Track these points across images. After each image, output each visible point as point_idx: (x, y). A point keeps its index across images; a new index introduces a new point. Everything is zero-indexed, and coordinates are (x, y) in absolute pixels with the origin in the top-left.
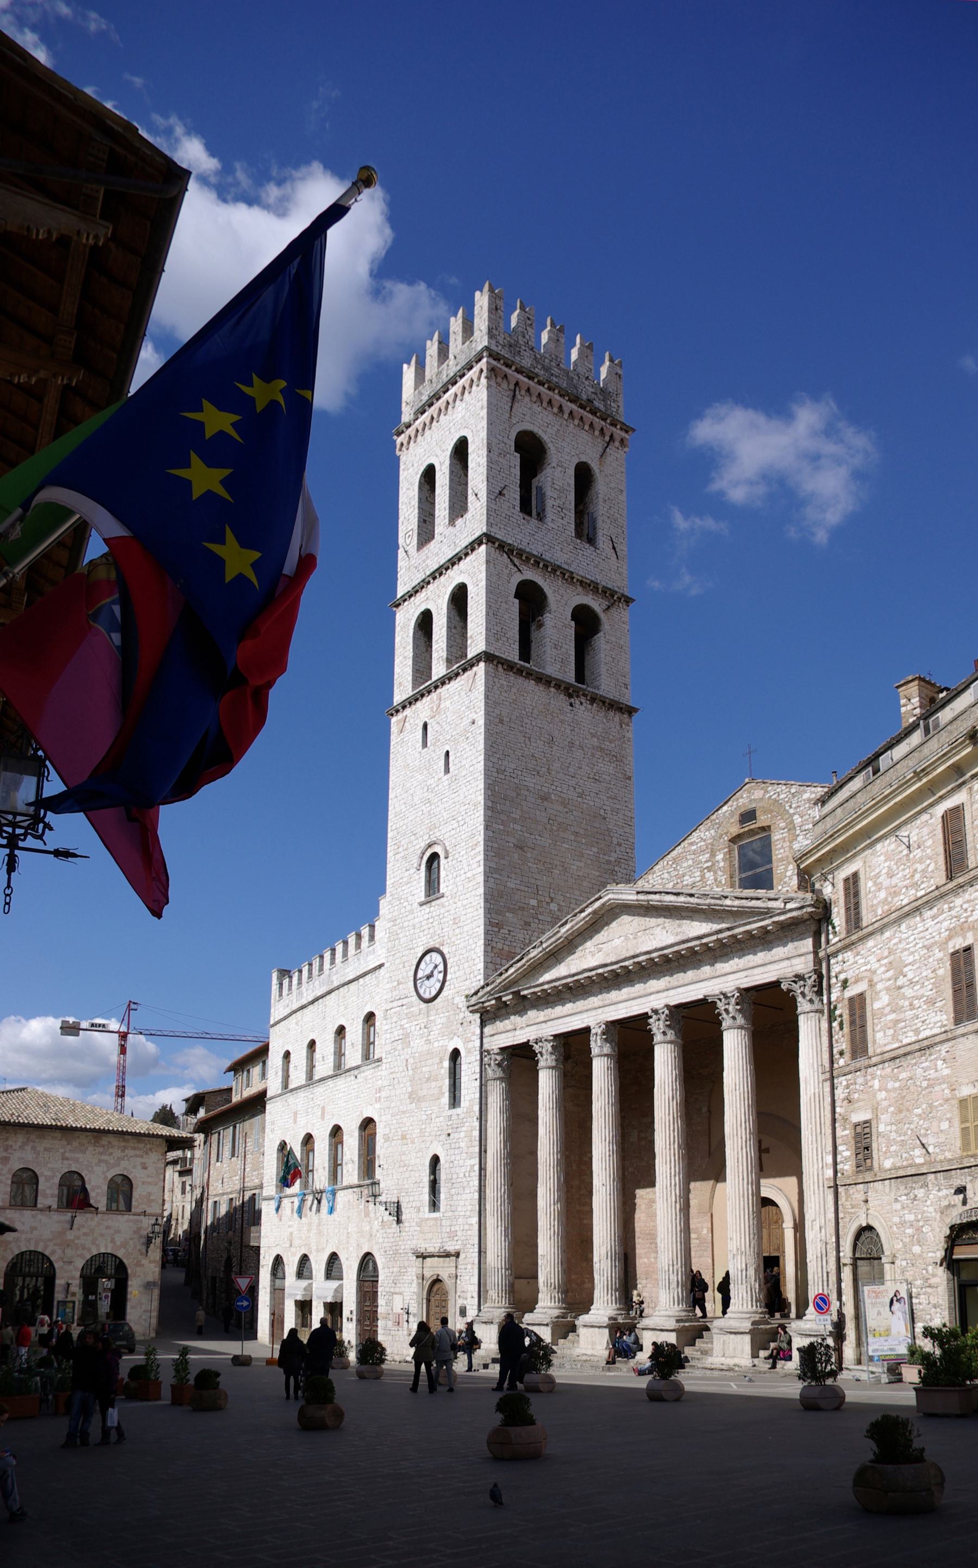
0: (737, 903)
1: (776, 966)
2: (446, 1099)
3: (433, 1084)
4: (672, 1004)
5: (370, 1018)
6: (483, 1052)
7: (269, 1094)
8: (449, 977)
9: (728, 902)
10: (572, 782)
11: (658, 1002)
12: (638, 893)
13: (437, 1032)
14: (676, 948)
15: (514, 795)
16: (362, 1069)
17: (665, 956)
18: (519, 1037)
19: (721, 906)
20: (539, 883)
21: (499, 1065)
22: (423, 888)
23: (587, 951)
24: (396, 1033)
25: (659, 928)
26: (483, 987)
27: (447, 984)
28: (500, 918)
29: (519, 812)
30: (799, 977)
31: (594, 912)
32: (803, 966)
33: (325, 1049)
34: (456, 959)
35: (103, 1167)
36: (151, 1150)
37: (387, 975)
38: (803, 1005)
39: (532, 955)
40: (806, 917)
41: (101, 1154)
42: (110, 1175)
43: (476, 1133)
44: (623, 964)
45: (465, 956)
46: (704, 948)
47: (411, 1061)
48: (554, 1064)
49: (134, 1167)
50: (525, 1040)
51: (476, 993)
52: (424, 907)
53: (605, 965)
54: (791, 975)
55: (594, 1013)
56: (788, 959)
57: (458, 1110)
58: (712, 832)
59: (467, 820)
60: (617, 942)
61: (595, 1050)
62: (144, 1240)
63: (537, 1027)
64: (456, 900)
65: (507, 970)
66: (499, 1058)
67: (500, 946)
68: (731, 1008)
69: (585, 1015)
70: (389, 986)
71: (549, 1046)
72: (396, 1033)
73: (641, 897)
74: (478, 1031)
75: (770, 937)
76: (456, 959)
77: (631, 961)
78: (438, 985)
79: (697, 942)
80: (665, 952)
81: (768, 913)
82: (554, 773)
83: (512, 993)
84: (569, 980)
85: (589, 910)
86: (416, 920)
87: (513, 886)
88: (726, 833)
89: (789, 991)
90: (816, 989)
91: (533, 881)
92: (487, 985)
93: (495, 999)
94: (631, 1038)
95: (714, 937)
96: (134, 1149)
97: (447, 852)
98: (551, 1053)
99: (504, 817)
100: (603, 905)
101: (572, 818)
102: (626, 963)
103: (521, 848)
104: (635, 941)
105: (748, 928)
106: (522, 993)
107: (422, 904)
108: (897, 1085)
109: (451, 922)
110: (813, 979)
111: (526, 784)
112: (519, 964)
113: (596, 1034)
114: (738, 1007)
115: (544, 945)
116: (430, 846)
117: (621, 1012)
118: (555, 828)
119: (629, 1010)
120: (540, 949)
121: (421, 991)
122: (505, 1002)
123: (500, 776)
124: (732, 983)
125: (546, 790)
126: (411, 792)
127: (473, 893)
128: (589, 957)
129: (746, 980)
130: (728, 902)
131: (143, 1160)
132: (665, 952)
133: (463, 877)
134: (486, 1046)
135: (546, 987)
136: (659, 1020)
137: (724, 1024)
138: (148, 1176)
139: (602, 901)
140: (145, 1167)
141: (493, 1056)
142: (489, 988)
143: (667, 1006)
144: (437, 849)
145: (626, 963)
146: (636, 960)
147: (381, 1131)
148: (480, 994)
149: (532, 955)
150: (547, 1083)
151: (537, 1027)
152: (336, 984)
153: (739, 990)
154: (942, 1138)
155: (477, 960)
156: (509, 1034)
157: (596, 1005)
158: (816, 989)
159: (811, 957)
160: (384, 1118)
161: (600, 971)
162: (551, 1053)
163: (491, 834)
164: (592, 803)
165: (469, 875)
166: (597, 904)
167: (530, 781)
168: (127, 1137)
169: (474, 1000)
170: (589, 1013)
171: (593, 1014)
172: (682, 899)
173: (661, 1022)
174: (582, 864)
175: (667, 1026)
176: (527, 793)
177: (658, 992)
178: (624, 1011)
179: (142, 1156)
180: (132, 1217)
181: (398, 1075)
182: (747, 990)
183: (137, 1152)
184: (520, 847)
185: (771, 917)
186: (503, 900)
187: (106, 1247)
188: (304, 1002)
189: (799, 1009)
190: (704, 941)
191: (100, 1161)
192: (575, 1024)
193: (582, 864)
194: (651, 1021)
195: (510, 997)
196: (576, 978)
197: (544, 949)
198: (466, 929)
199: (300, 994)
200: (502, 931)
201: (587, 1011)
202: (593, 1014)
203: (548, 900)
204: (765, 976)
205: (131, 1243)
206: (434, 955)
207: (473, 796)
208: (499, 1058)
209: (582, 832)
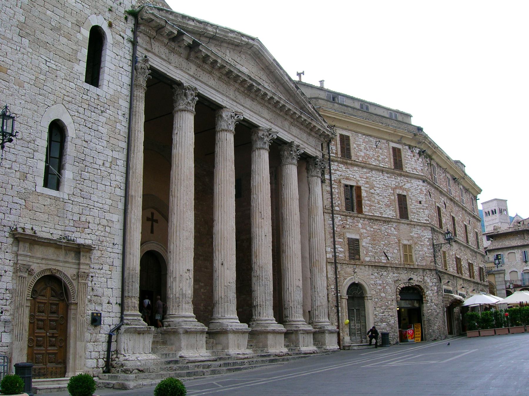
2: (82, 67)
3: (64, 40)
18: (175, 73)
19: (307, 105)
31: (247, 44)
50: (178, 79)
55: (231, 102)
69: (225, 98)
83: (194, 41)
84: (235, 72)
102: (269, 93)
105: (317, 125)
106: (200, 48)
108: (372, 229)
119: (251, 117)
135: (219, 61)
154: (394, 255)
156: (164, 63)
170: (228, 100)
178: (248, 115)
196: (239, 74)
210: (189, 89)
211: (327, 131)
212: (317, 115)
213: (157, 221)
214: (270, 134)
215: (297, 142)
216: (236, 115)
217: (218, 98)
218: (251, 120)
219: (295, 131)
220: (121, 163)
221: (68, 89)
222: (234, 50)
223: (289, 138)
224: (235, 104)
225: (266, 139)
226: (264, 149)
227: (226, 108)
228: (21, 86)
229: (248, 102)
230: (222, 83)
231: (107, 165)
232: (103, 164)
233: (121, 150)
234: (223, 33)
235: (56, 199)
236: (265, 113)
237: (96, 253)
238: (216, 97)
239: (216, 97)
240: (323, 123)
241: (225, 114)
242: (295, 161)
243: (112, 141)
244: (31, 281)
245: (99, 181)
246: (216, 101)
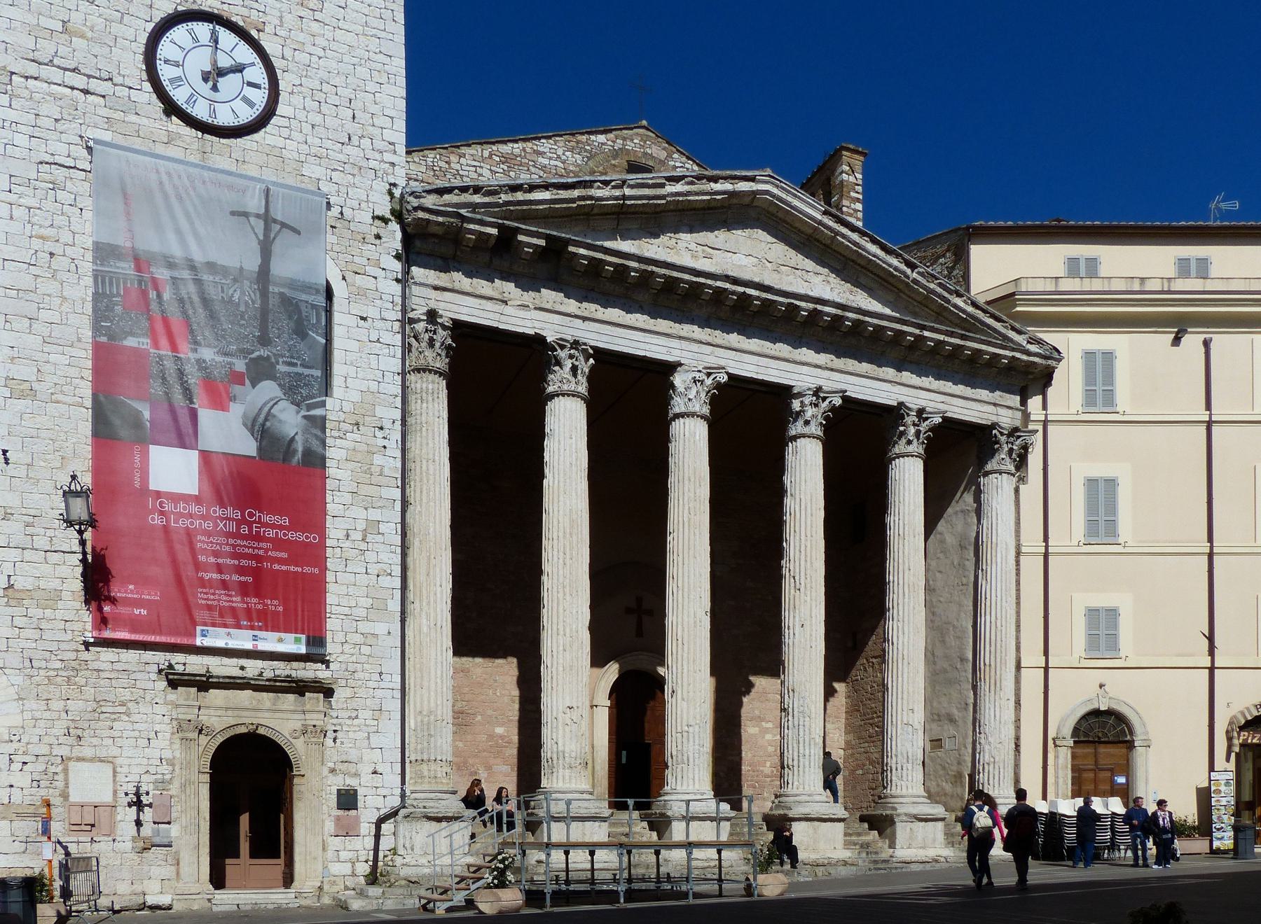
9: (959, 302)
19: (948, 301)
25: (821, 278)
55: (695, 347)
60: (740, 259)
69: (675, 343)
77: (811, 306)
79: (917, 331)
81: (1006, 342)
95: (941, 337)
104: (775, 275)
105: (984, 347)
130: (959, 302)
145: (803, 304)
146: (819, 307)
170: (685, 344)
190: (926, 334)
201: (680, 338)
210: (562, 347)
211: (1028, 353)
212: (990, 321)
214: (824, 399)
215: (914, 399)
216: (709, 375)
217: (654, 348)
218: (760, 377)
223: (894, 396)
225: (810, 412)
226: (804, 436)
227: (681, 365)
231: (359, 536)
232: (348, 536)
233: (389, 504)
238: (647, 347)
239: (647, 347)
240: (1012, 334)
241: (679, 380)
242: (916, 448)
243: (365, 490)
245: (341, 568)
246: (649, 354)
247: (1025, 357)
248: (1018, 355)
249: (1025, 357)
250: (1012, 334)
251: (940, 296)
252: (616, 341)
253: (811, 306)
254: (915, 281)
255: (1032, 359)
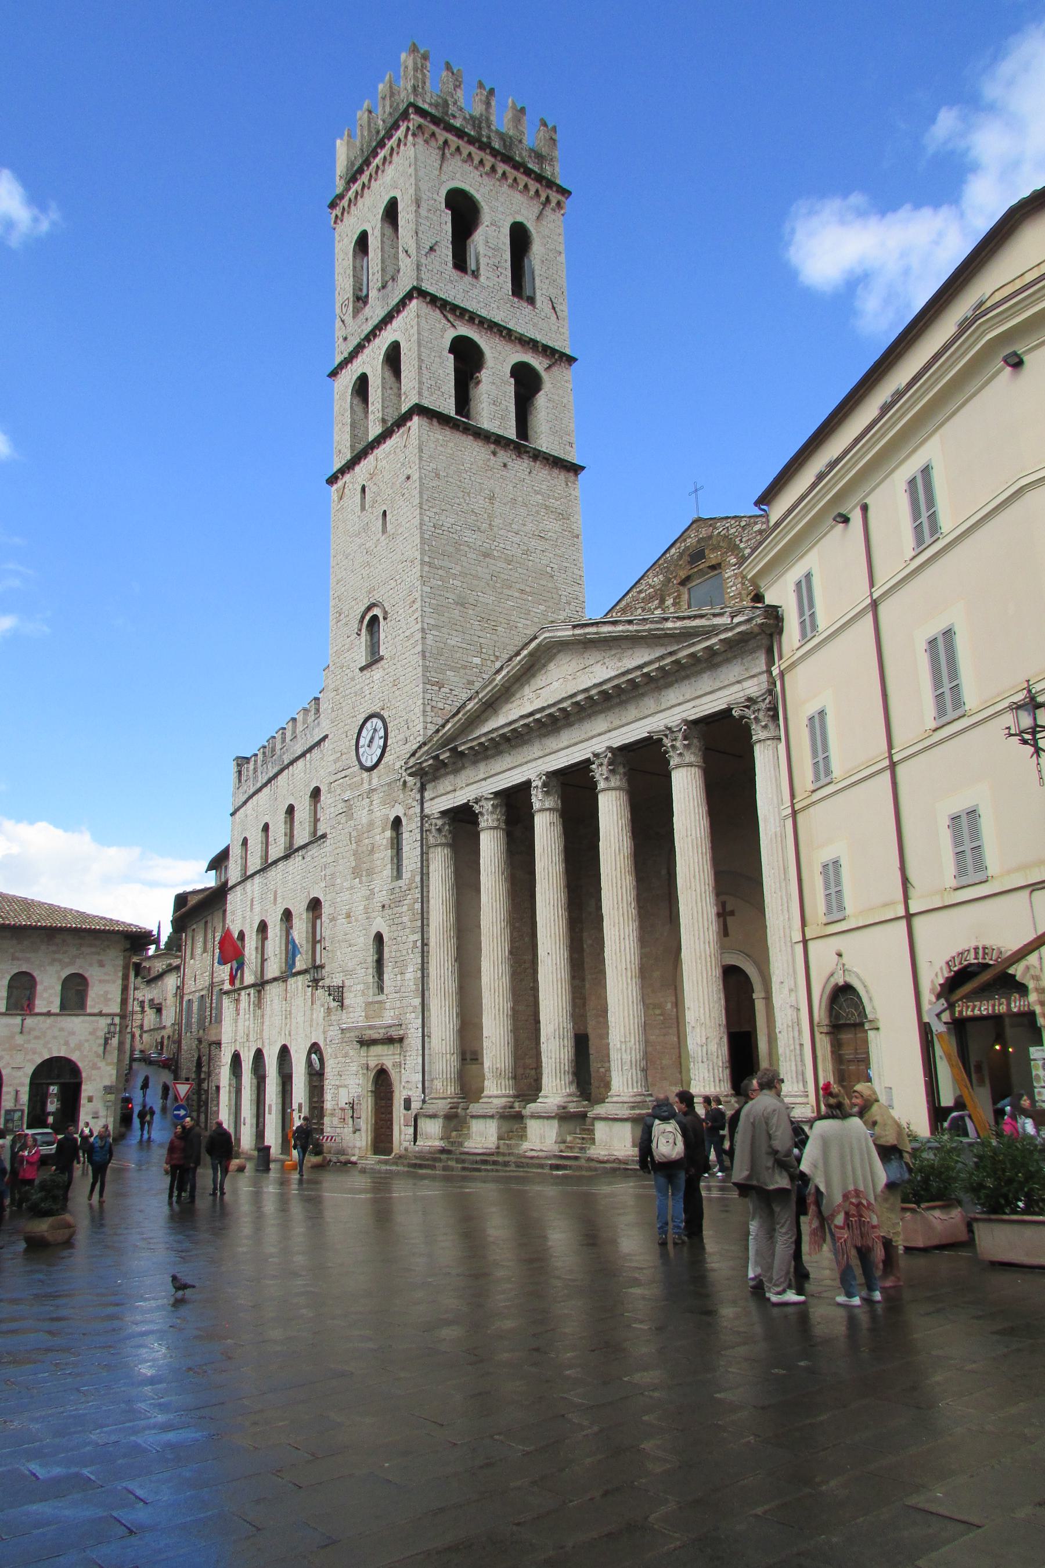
0: (679, 624)
1: (726, 692)
4: (615, 746)
5: (316, 793)
6: (423, 817)
7: (230, 884)
8: (389, 742)
9: (669, 625)
10: (517, 539)
11: (599, 746)
12: (574, 627)
13: (378, 801)
14: (616, 682)
15: (451, 549)
16: (309, 847)
17: (603, 693)
19: (663, 629)
20: (482, 640)
21: (439, 830)
22: (364, 654)
23: (526, 698)
24: (339, 806)
26: (420, 747)
27: (388, 749)
28: (441, 676)
29: (459, 568)
30: (751, 701)
31: (531, 654)
32: (755, 689)
33: (278, 830)
34: (395, 722)
35: (57, 967)
36: (108, 946)
37: (331, 747)
38: (758, 733)
39: (468, 707)
40: (757, 630)
41: (55, 952)
42: (64, 975)
43: (418, 906)
44: (561, 706)
45: (405, 718)
46: (645, 680)
47: (354, 834)
48: (495, 824)
49: (91, 965)
51: (413, 754)
52: (365, 672)
53: (543, 709)
54: (743, 700)
55: (534, 764)
56: (738, 682)
57: (401, 883)
58: (661, 577)
59: (405, 577)
61: (536, 805)
62: (102, 1041)
63: (477, 786)
64: (396, 661)
65: (443, 726)
66: (440, 822)
67: (440, 705)
68: (678, 744)
69: (525, 768)
70: (332, 758)
71: (488, 805)
72: (339, 806)
73: (578, 631)
74: (418, 797)
75: (719, 659)
76: (395, 722)
77: (569, 702)
78: (379, 751)
79: (639, 673)
80: (604, 687)
82: (495, 529)
84: (506, 730)
85: (525, 652)
86: (358, 687)
87: (453, 643)
88: (675, 577)
89: (743, 717)
90: (771, 713)
91: (476, 639)
92: (425, 744)
93: (432, 758)
94: (574, 788)
95: (657, 665)
96: (91, 946)
97: (386, 613)
98: (492, 813)
99: (440, 572)
100: (539, 645)
101: (517, 575)
103: (462, 605)
104: (574, 682)
105: (692, 650)
107: (362, 669)
109: (390, 685)
110: (767, 701)
111: (466, 539)
112: (456, 719)
113: (537, 787)
114: (686, 742)
115: (480, 696)
116: (369, 609)
117: (562, 760)
118: (498, 585)
119: (570, 757)
120: (476, 700)
121: (363, 760)
122: (442, 761)
123: (438, 531)
124: (679, 717)
125: (488, 546)
126: (351, 557)
127: (412, 652)
128: (527, 704)
129: (693, 711)
130: (669, 625)
131: (100, 958)
132: (604, 687)
133: (402, 637)
134: (427, 811)
135: (483, 740)
136: (601, 765)
137: (672, 763)
138: (105, 974)
139: (537, 641)
140: (101, 965)
141: (434, 821)
142: (426, 748)
143: (610, 749)
144: (376, 611)
146: (574, 700)
147: (326, 910)
148: (417, 755)
149: (468, 707)
150: (490, 846)
151: (477, 786)
152: (286, 763)
153: (686, 722)
155: (417, 721)
157: (535, 756)
158: (771, 713)
159: (764, 677)
160: (328, 897)
161: (538, 716)
162: (492, 813)
163: (429, 589)
164: (538, 560)
165: (407, 633)
166: (533, 645)
167: (469, 536)
168: (82, 934)
169: (412, 762)
171: (532, 766)
172: (620, 628)
173: (604, 767)
174: (528, 622)
175: (611, 771)
176: (467, 549)
177: (600, 735)
179: (99, 954)
180: (87, 1018)
181: (341, 850)
182: (696, 722)
183: (93, 950)
184: (462, 603)
185: (717, 634)
186: (443, 658)
187: (59, 1050)
188: (259, 785)
189: (754, 738)
190: (645, 670)
191: (54, 960)
192: (514, 778)
193: (528, 622)
194: (593, 766)
195: (448, 754)
196: (513, 727)
197: (480, 700)
198: (405, 689)
199: (255, 778)
200: (443, 690)
201: (526, 763)
202: (532, 766)
203: (492, 658)
204: (714, 704)
205: (86, 1045)
206: (375, 720)
207: (410, 552)
208: (440, 822)
209: (528, 589)
213: (732, 913)
219: (672, 696)
220: (419, 944)
221: (381, 899)
222: (534, 676)
224: (540, 762)
228: (357, 920)
229: (566, 737)
230: (520, 749)
234: (489, 688)
235: (380, 1002)
236: (599, 724)
237: (406, 1042)
240: (717, 621)
244: (372, 1074)
247: (730, 634)
248: (722, 636)
249: (730, 634)
250: (717, 621)
251: (656, 629)
252: (502, 783)
253: (569, 702)
254: (636, 631)
255: (738, 630)
